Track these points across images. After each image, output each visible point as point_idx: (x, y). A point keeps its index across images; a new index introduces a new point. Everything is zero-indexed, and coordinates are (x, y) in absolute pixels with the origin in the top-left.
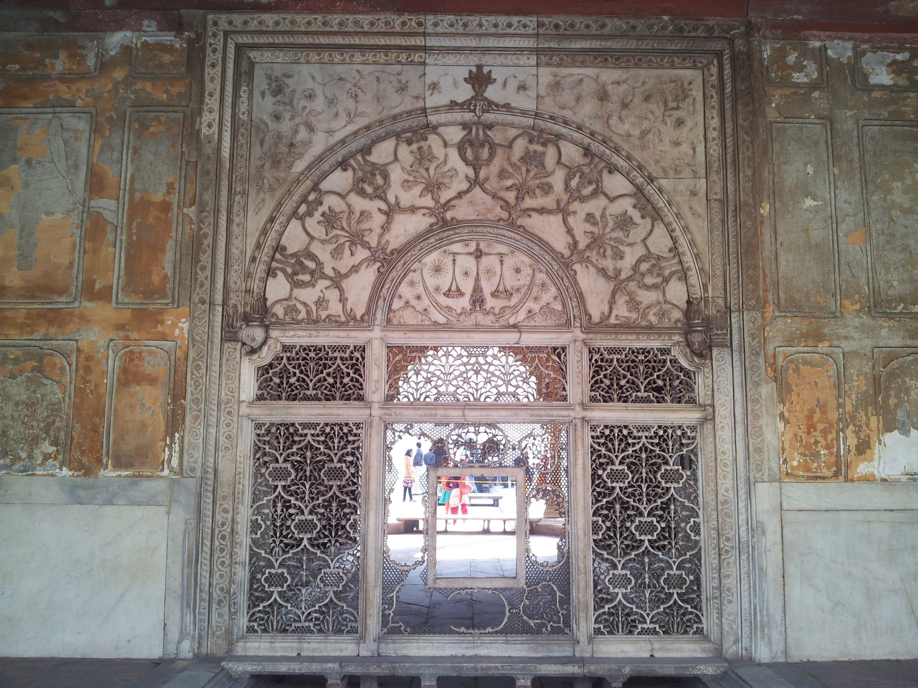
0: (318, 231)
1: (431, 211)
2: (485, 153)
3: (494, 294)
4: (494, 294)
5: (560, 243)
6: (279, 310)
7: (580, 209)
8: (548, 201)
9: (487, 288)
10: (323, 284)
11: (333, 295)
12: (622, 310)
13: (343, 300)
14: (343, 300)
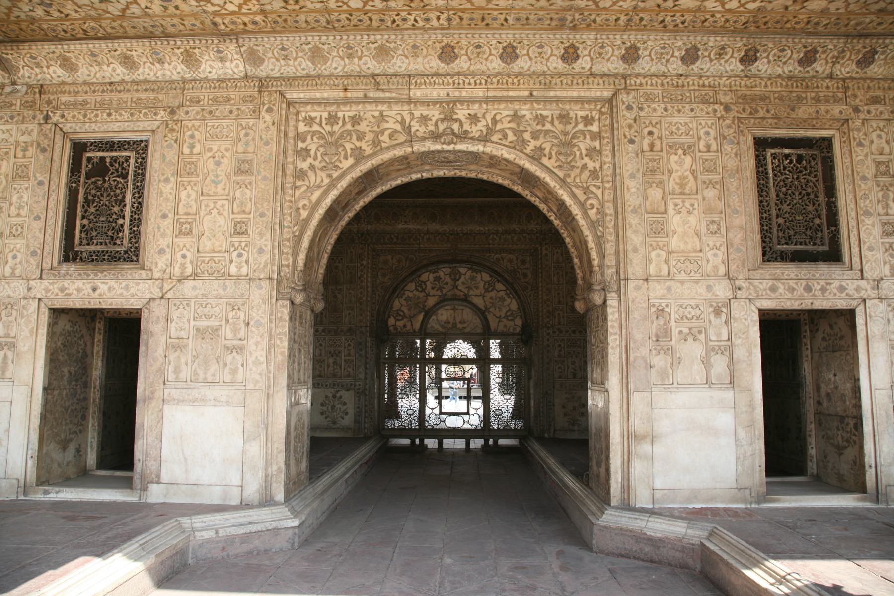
0: (404, 303)
1: (440, 296)
2: (458, 277)
3: (460, 322)
4: (460, 322)
5: (482, 306)
6: (391, 328)
7: (489, 295)
8: (478, 292)
9: (458, 320)
10: (405, 320)
11: (409, 324)
12: (501, 328)
13: (412, 325)
14: (412, 325)
